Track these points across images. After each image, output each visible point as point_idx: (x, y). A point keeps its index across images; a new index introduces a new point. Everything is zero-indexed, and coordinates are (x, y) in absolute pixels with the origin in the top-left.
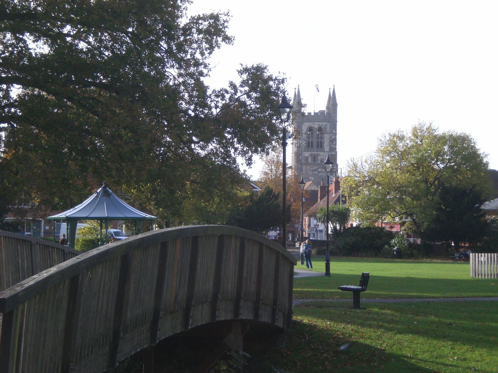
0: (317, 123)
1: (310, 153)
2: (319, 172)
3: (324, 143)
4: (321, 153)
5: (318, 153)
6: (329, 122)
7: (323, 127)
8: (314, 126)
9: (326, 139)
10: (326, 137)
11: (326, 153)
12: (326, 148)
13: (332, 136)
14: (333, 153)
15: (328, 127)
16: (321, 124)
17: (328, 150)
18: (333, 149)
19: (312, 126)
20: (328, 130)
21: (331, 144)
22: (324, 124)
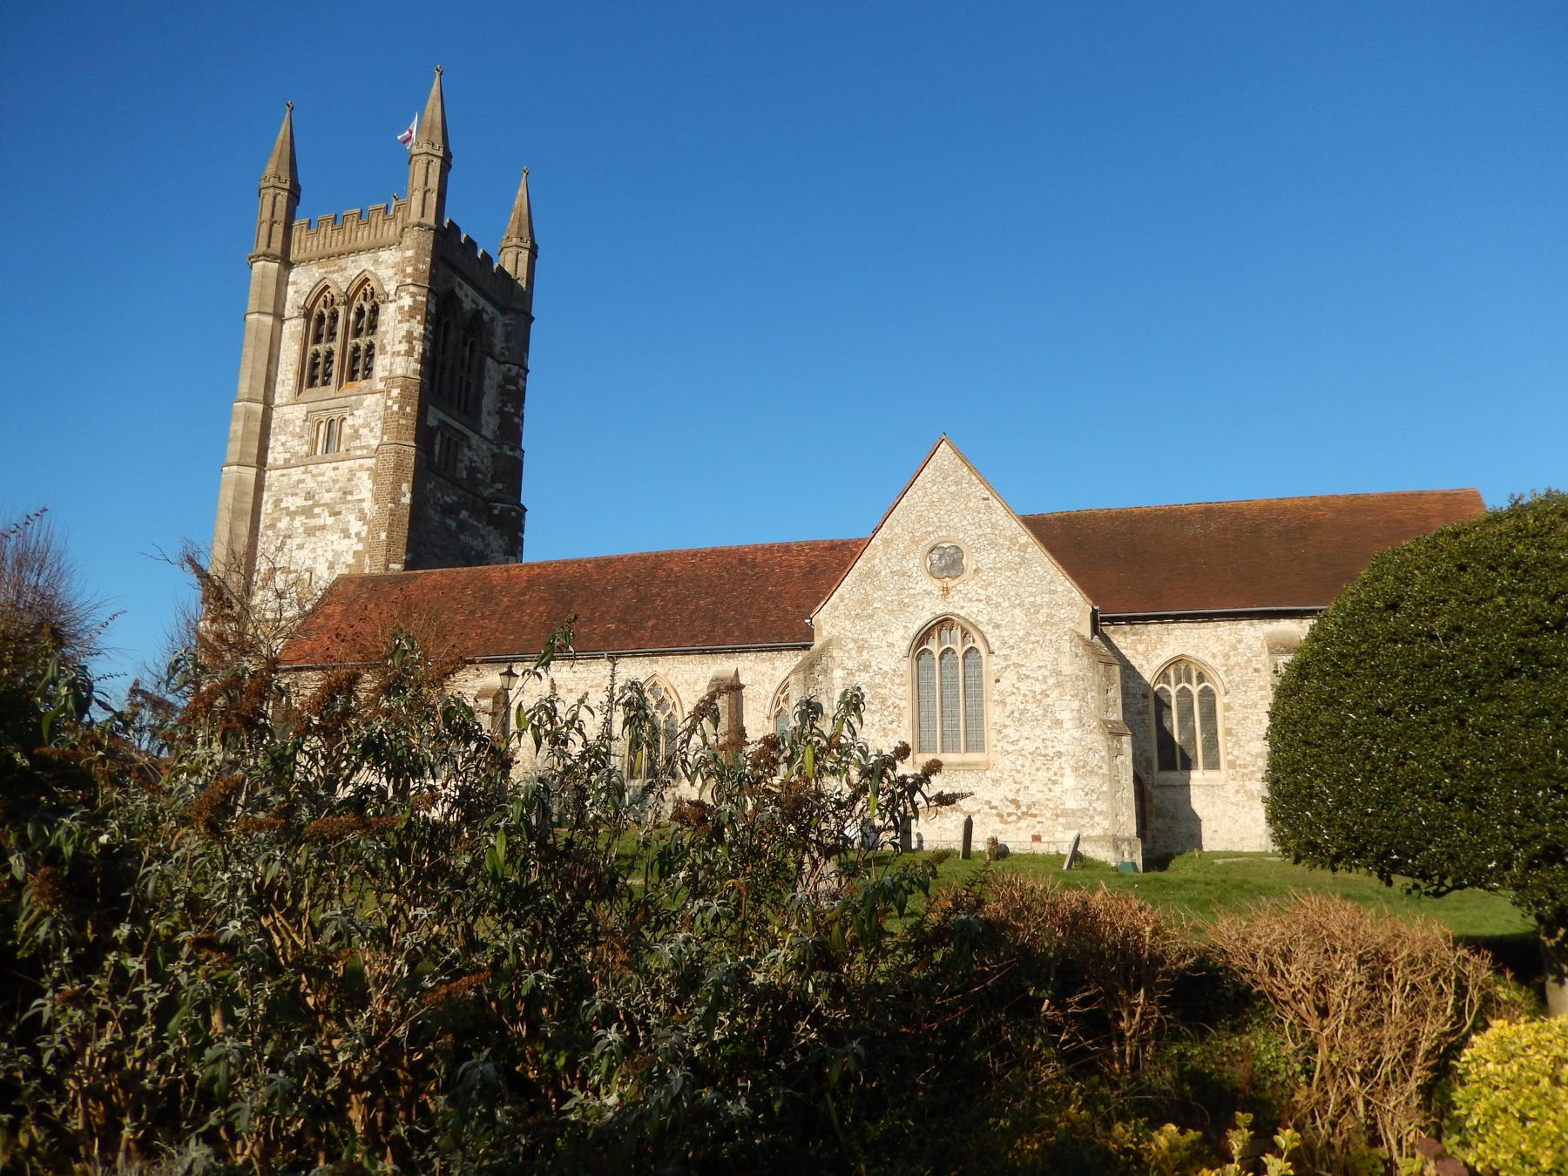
0: (471, 292)
1: (441, 415)
2: (463, 526)
3: (479, 395)
4: (474, 438)
5: (470, 433)
6: (504, 310)
7: (486, 317)
8: (461, 294)
9: (487, 382)
10: (494, 372)
11: (484, 446)
12: (490, 424)
13: (518, 375)
14: (517, 454)
15: (499, 330)
16: (482, 302)
17: (489, 435)
18: (511, 431)
19: (457, 290)
20: (498, 343)
21: (509, 409)
22: (490, 308)
